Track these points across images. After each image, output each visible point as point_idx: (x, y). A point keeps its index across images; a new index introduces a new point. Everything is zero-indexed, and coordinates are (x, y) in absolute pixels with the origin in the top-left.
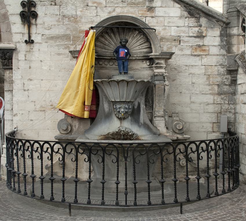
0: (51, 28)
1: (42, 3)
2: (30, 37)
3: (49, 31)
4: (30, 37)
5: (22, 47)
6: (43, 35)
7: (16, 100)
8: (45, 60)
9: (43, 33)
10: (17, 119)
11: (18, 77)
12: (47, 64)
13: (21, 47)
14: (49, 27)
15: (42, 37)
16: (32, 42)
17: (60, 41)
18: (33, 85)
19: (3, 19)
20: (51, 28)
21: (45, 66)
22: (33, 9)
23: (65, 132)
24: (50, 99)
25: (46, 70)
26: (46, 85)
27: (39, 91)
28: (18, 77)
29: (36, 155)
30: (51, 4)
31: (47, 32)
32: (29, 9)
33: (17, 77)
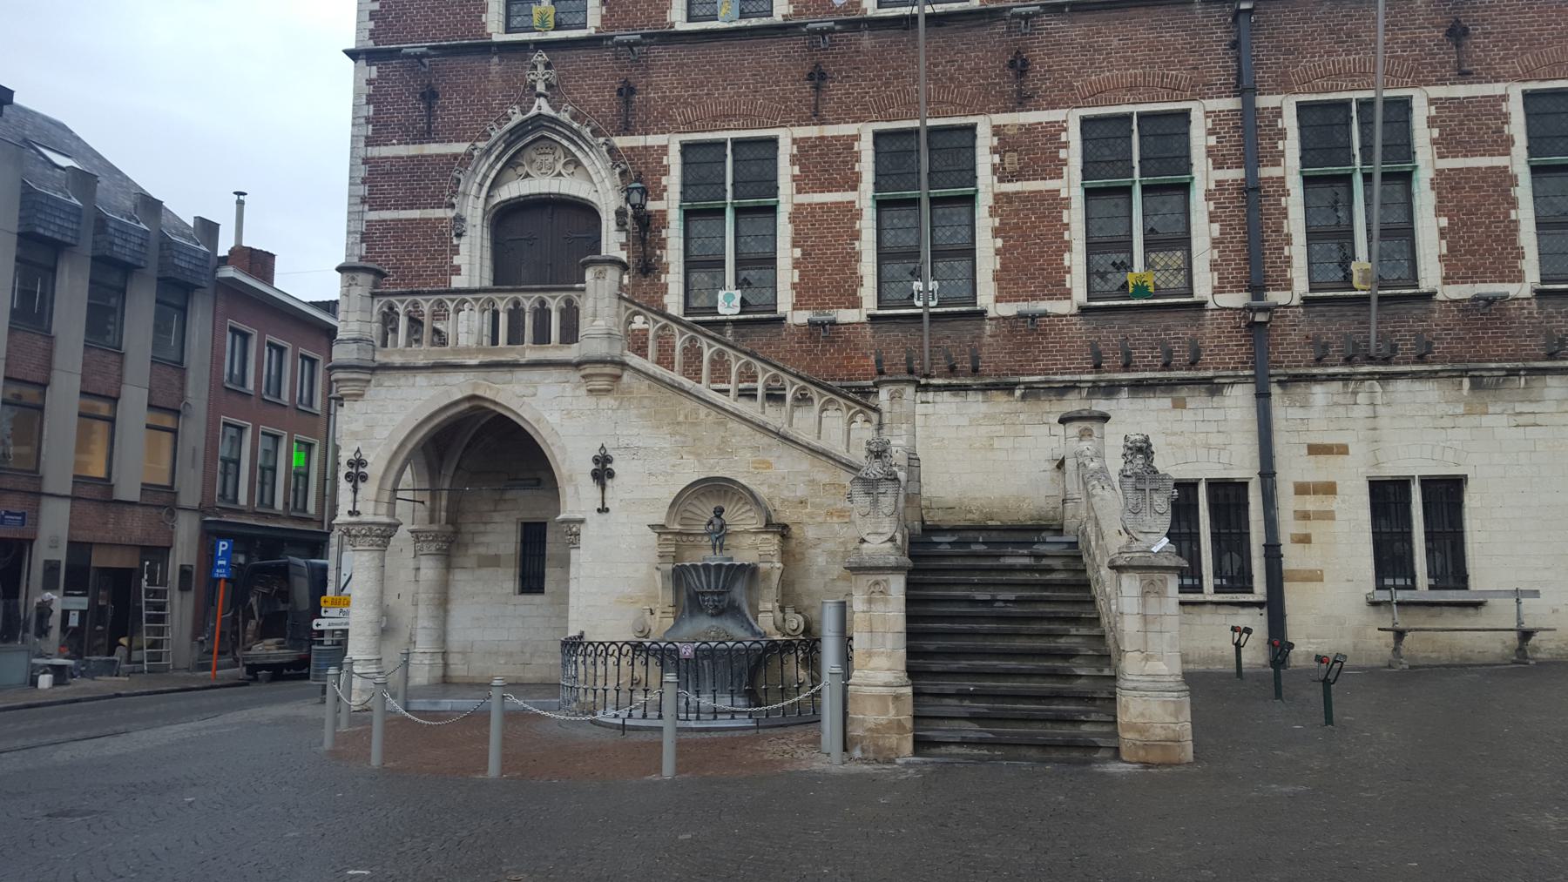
2: (603, 504)
4: (603, 504)
5: (593, 518)
22: (609, 466)
23: (638, 635)
29: (600, 660)
31: (627, 496)
32: (604, 466)
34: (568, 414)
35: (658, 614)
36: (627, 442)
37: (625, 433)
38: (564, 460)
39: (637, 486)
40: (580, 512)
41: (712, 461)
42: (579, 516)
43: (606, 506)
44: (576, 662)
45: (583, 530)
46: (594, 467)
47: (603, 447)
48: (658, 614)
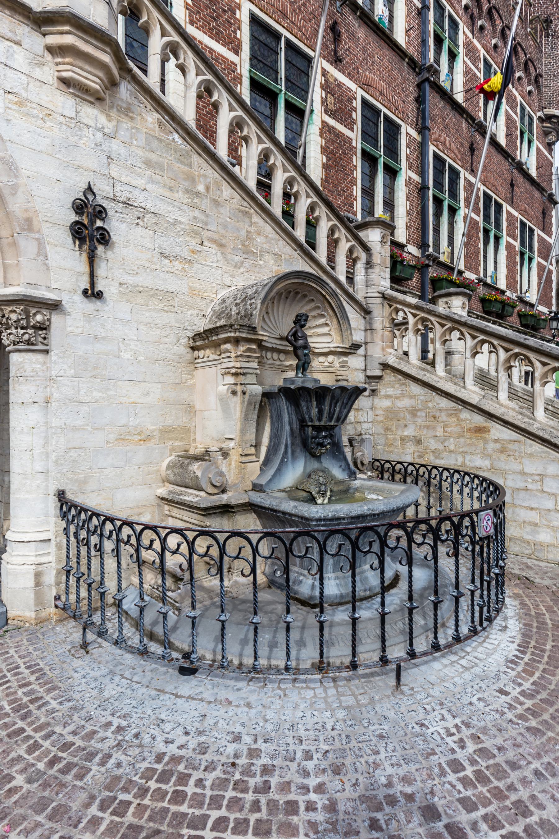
0: (137, 273)
1: (118, 214)
2: (93, 284)
3: (133, 278)
4: (93, 284)
6: (121, 284)
7: (61, 426)
8: (125, 337)
9: (121, 280)
10: (65, 470)
11: (65, 373)
12: (131, 347)
13: (73, 303)
14: (134, 271)
15: (121, 289)
16: (99, 295)
17: (154, 304)
18: (100, 391)
19: (26, 227)
20: (137, 273)
21: (126, 351)
24: (138, 421)
25: (128, 359)
26: (128, 391)
27: (114, 405)
28: (65, 373)
30: (138, 224)
31: (130, 279)
33: (62, 371)
34: (20, 104)
35: (234, 457)
36: (126, 194)
37: (124, 179)
38: (14, 188)
39: (145, 268)
40: (50, 289)
41: (236, 258)
42: (51, 296)
43: (99, 287)
44: (100, 549)
45: (56, 319)
46: (74, 218)
47: (90, 189)
48: (234, 457)
